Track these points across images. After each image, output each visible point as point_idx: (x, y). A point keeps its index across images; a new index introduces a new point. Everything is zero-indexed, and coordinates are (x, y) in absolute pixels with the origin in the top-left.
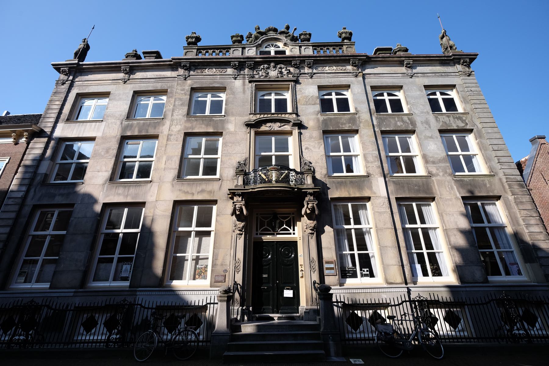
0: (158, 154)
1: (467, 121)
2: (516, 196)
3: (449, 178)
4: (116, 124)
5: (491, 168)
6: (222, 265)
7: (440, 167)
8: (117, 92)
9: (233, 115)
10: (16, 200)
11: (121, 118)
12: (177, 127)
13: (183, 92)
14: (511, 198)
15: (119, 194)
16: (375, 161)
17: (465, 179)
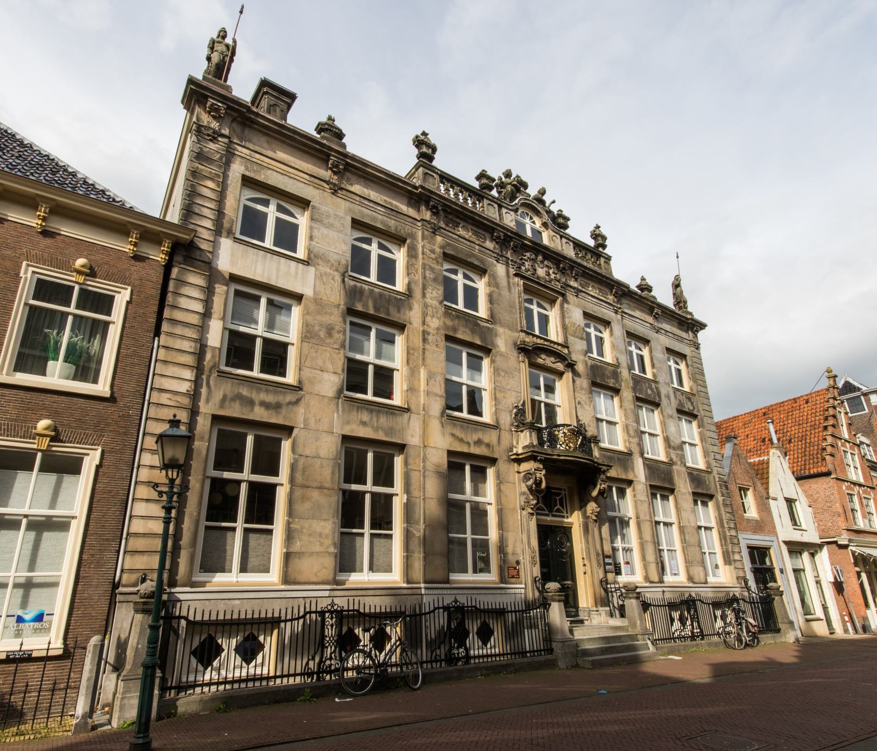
0: (411, 362)
4: (333, 279)
5: (708, 465)
6: (513, 554)
8: (323, 208)
9: (502, 325)
10: (179, 398)
11: (342, 270)
12: (434, 320)
13: (433, 256)
14: (720, 499)
15: (364, 423)
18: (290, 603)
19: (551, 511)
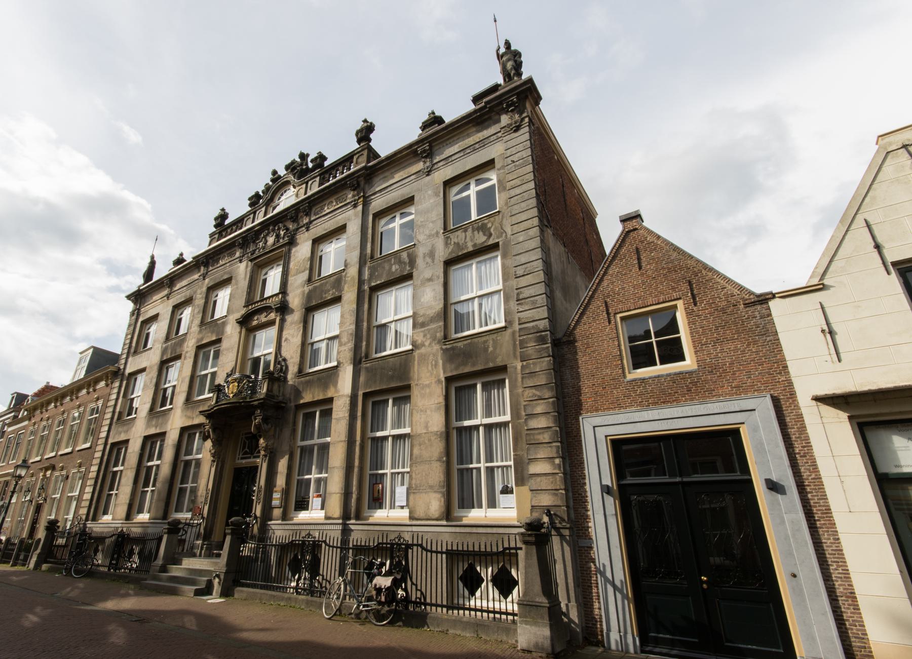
1: (492, 230)
2: (525, 363)
3: (436, 347)
7: (429, 330)
16: (349, 342)
17: (460, 344)
18: (490, 538)
19: (252, 454)
